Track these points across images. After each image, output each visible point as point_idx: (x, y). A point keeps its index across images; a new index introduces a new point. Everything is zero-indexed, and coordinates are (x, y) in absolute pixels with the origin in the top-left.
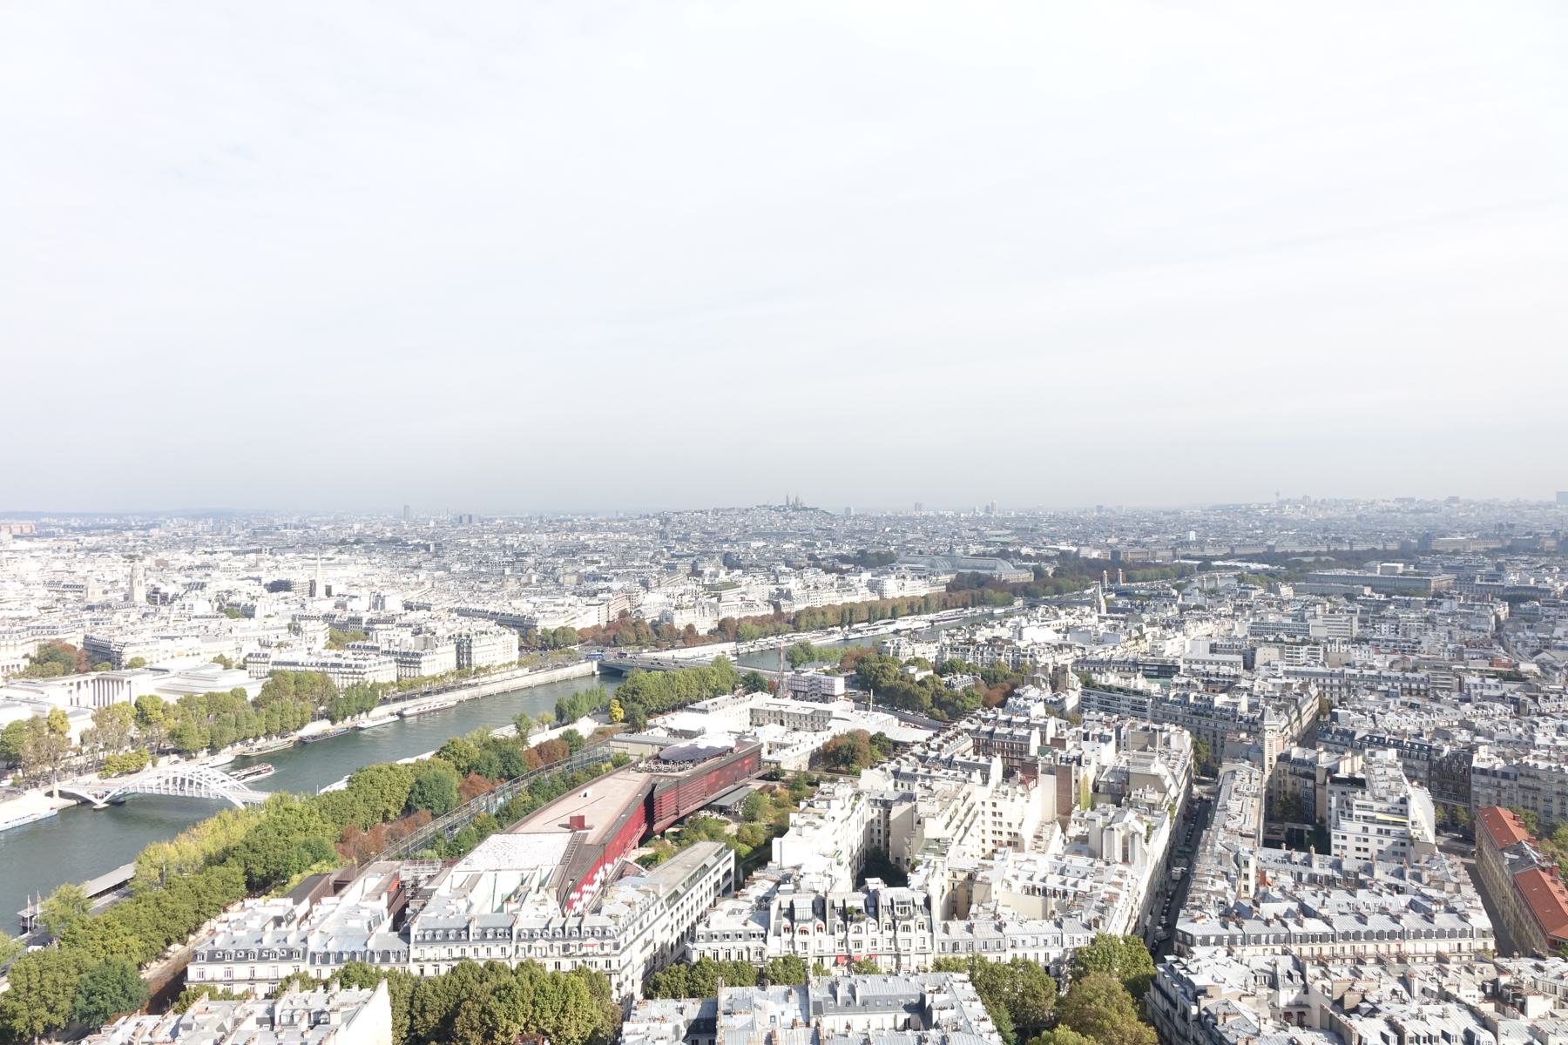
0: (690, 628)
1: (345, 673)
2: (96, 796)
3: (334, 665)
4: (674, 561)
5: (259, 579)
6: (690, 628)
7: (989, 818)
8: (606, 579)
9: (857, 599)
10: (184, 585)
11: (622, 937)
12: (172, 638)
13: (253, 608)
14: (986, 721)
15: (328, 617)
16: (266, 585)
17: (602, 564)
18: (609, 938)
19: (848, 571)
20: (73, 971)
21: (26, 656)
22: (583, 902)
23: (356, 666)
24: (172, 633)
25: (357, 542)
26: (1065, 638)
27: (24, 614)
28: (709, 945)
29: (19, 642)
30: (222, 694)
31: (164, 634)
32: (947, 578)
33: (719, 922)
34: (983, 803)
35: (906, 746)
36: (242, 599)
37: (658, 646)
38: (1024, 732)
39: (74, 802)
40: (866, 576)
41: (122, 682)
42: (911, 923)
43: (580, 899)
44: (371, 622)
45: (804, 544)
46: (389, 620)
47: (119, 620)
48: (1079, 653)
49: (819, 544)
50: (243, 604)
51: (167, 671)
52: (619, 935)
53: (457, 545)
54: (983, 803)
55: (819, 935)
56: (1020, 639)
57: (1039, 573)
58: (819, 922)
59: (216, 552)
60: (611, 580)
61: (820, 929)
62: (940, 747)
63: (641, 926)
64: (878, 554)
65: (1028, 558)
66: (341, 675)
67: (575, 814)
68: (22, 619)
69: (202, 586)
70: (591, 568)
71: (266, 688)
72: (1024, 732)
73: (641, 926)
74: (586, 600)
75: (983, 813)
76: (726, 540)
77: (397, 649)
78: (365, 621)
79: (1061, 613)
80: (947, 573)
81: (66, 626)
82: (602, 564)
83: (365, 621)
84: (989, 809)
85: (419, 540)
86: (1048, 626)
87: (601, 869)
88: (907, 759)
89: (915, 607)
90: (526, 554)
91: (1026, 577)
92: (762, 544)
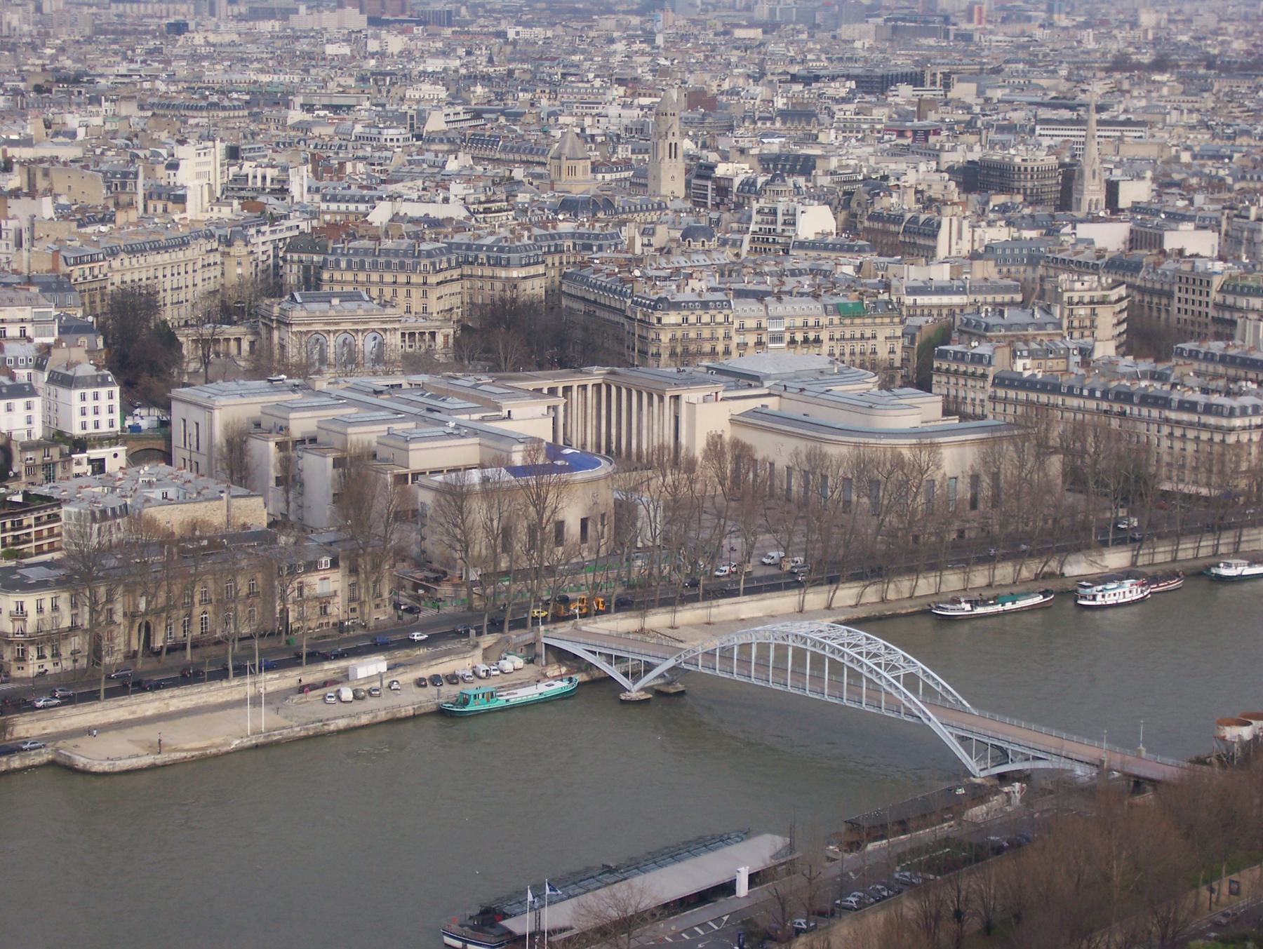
1: (1178, 423)
3: (1148, 400)
10: (766, 162)
13: (932, 231)
15: (1119, 266)
16: (950, 170)
23: (1209, 409)
27: (437, 211)
29: (433, 279)
36: (901, 203)
41: (661, 398)
47: (632, 240)
50: (908, 216)
51: (756, 378)
59: (817, 78)
66: (1166, 430)
68: (435, 223)
78: (1217, 282)
83: (1217, 282)
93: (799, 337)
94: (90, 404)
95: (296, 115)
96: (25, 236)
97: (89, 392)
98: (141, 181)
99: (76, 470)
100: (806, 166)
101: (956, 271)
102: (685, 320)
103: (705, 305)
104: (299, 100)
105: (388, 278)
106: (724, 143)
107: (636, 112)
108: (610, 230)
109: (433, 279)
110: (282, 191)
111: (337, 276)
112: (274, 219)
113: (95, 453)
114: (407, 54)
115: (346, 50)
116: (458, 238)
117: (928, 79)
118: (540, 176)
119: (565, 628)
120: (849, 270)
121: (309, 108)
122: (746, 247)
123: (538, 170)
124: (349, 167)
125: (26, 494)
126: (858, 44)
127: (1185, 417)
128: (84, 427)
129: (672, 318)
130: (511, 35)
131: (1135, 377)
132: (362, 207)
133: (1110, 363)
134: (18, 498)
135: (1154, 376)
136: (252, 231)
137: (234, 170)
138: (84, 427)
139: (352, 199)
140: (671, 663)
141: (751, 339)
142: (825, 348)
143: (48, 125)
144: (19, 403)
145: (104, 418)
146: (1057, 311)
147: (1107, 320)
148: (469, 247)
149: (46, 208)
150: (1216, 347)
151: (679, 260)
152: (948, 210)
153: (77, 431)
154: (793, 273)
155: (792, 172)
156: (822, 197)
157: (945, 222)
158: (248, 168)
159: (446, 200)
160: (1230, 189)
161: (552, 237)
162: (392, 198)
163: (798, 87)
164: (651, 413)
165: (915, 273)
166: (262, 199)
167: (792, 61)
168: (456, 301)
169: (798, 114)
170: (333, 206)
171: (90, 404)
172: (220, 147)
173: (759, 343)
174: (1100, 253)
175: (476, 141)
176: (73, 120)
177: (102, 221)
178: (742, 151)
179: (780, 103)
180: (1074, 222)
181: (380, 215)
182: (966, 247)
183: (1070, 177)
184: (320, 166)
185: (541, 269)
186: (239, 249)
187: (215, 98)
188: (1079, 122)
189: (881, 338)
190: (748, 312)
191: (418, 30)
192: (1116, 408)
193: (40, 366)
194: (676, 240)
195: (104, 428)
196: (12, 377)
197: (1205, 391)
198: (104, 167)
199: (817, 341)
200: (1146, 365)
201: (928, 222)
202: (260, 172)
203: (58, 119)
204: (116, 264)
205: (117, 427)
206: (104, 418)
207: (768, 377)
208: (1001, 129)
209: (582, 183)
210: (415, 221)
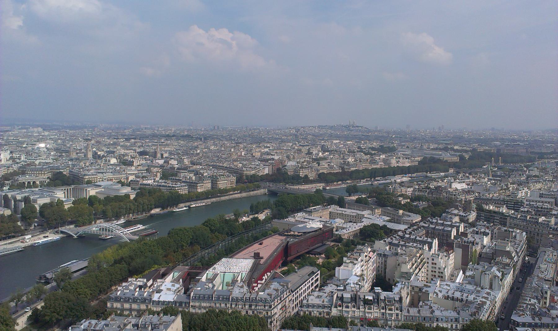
0: (306, 176)
2: (74, 233)
3: (163, 186)
4: (301, 147)
5: (135, 150)
6: (306, 176)
7: (430, 265)
8: (272, 155)
9: (378, 166)
10: (107, 152)
11: (273, 303)
12: (102, 173)
13: (133, 162)
14: (432, 223)
15: (161, 166)
17: (271, 148)
18: (268, 303)
19: (375, 154)
20: (66, 301)
21: (48, 178)
22: (258, 287)
23: (172, 187)
24: (102, 171)
26: (471, 188)
28: (308, 309)
29: (46, 172)
30: (120, 196)
31: (100, 171)
32: (419, 159)
33: (312, 300)
34: (428, 259)
35: (396, 231)
36: (129, 158)
37: (293, 184)
38: (450, 229)
39: (65, 236)
40: (383, 156)
42: (393, 307)
43: (257, 286)
44: (178, 169)
45: (356, 142)
46: (186, 168)
47: (82, 165)
48: (477, 194)
49: (363, 142)
52: (271, 302)
53: (213, 138)
54: (428, 259)
55: (353, 309)
56: (450, 187)
57: (462, 158)
58: (354, 304)
60: (274, 155)
61: (354, 307)
62: (410, 233)
63: (280, 299)
64: (389, 147)
65: (457, 151)
67: (256, 252)
68: (47, 163)
69: (114, 152)
70: (266, 150)
71: (137, 195)
72: (450, 229)
73: (280, 299)
74: (264, 163)
75: (428, 263)
76: (323, 139)
77: (188, 181)
78: (176, 168)
79: (471, 177)
80: (419, 156)
81: (63, 167)
82: (271, 148)
83: (176, 168)
84: (430, 261)
86: (464, 182)
87: (266, 274)
88: (395, 237)
89: (403, 171)
90: (240, 143)
91: (456, 159)
92: (338, 141)
93: (109, 179)
95: (24, 146)
100: (113, 152)
105: (38, 172)
108: (78, 163)
110: (20, 159)
111: (28, 172)
116: (51, 165)
117: (137, 138)
120: (118, 168)
121: (27, 144)
124: (33, 154)
127: (169, 188)
129: (87, 177)
131: (161, 183)
132: (35, 161)
133: (158, 181)
135: (165, 182)
136: (14, 165)
137: (11, 155)
139: (33, 160)
141: (101, 180)
146: (151, 173)
147: (159, 174)
148: (53, 167)
155: (111, 153)
158: (14, 155)
159: (49, 159)
161: (68, 165)
162: (39, 159)
163: (115, 140)
164: (82, 192)
166: (16, 160)
170: (29, 161)
172: (9, 152)
173: (102, 181)
174: (159, 164)
180: (156, 160)
181: (37, 162)
185: (65, 170)
186: (11, 168)
190: (100, 176)
197: (172, 184)
199: (112, 180)
200: (164, 181)
201: (132, 161)
207: (102, 185)
209: (74, 156)
210: (43, 163)
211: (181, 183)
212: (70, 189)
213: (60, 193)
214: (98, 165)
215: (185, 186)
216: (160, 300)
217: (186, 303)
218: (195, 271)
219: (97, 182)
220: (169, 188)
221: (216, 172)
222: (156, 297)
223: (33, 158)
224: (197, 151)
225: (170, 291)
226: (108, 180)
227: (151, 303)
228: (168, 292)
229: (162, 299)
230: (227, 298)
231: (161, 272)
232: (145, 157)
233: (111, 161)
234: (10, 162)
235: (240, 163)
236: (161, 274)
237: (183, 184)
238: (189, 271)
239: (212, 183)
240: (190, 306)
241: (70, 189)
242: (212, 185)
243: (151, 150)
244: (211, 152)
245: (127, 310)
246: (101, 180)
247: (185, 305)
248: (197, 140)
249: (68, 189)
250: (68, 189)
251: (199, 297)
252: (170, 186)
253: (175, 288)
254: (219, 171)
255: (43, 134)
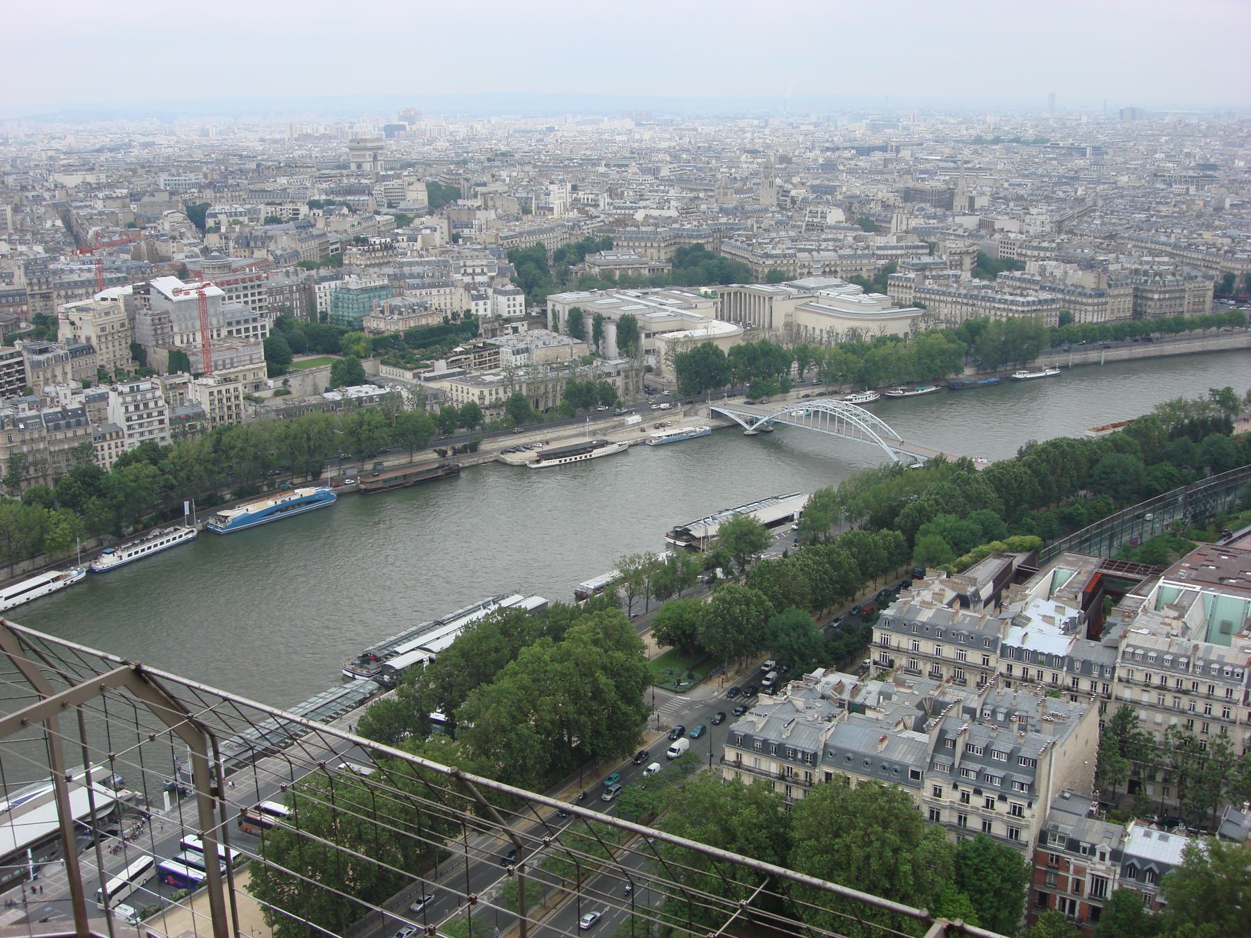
10: (814, 189)
12: (810, 251)
21: (669, 260)
23: (1012, 303)
25: (996, 141)
27: (666, 213)
36: (876, 208)
59: (838, 149)
66: (993, 312)
69: (835, 188)
78: (1018, 244)
85: (1071, 141)
93: (827, 269)
94: (512, 303)
95: (602, 169)
96: (484, 227)
97: (511, 297)
98: (534, 201)
99: (506, 332)
100: (831, 190)
101: (899, 239)
102: (776, 262)
103: (785, 256)
104: (604, 162)
106: (796, 180)
107: (755, 166)
109: (662, 245)
110: (596, 206)
111: (620, 243)
112: (592, 217)
113: (514, 325)
114: (652, 139)
115: (625, 138)
116: (674, 226)
118: (711, 196)
119: (720, 402)
121: (606, 165)
122: (804, 228)
123: (711, 194)
125: (484, 343)
126: (857, 132)
127: (1002, 306)
128: (509, 312)
129: (770, 262)
130: (700, 130)
131: (979, 288)
132: (631, 212)
134: (481, 345)
137: (575, 195)
138: (509, 312)
140: (767, 418)
141: (805, 271)
142: (839, 275)
143: (493, 176)
144: (481, 303)
145: (518, 309)
146: (944, 257)
147: (967, 262)
148: (679, 229)
149: (492, 215)
150: (1017, 274)
151: (773, 235)
152: (897, 210)
153: (505, 315)
154: (825, 240)
155: (826, 193)
156: (838, 205)
157: (895, 216)
158: (581, 195)
159: (669, 208)
160: (1026, 200)
162: (644, 207)
163: (829, 153)
165: (880, 241)
166: (587, 208)
167: (827, 141)
168: (673, 254)
169: (829, 166)
170: (619, 211)
171: (512, 303)
172: (569, 186)
175: (680, 180)
176: (504, 174)
177: (517, 220)
178: (803, 184)
179: (821, 161)
180: (953, 216)
181: (639, 216)
182: (904, 228)
183: (951, 194)
184: (612, 192)
187: (566, 162)
188: (957, 169)
189: (864, 270)
191: (657, 128)
192: (971, 302)
193: (490, 286)
194: (772, 225)
195: (518, 313)
196: (478, 291)
198: (517, 195)
199: (836, 272)
200: (986, 283)
202: (586, 196)
203: (497, 173)
204: (523, 239)
205: (524, 312)
206: (518, 309)
208: (922, 172)
210: (656, 219)
211: (1036, 291)
212: (729, 294)
213: (704, 305)
214: (794, 226)
215: (1053, 301)
216: (1025, 647)
217: (1102, 666)
218: (1119, 573)
219: (794, 278)
220: (1002, 306)
221: (1147, 263)
222: (1013, 638)
223: (628, 204)
224: (1076, 192)
225: (1053, 624)
226: (824, 272)
227: (998, 652)
228: (1045, 627)
229: (1029, 646)
230: (1233, 673)
231: (1015, 564)
232: (923, 205)
233: (829, 216)
234: (574, 214)
235: (1225, 236)
236: (1013, 569)
237: (1045, 296)
238: (1105, 571)
239: (1136, 296)
240: (1116, 680)
241: (729, 294)
242: (1135, 304)
243: (937, 183)
244: (1122, 197)
245: (926, 657)
246: (805, 271)
247: (1101, 675)
248: (1071, 154)
249: (722, 295)
250: (722, 295)
251: (1145, 656)
252: (1006, 300)
253: (1065, 619)
254: (1157, 259)
255: (637, 136)
